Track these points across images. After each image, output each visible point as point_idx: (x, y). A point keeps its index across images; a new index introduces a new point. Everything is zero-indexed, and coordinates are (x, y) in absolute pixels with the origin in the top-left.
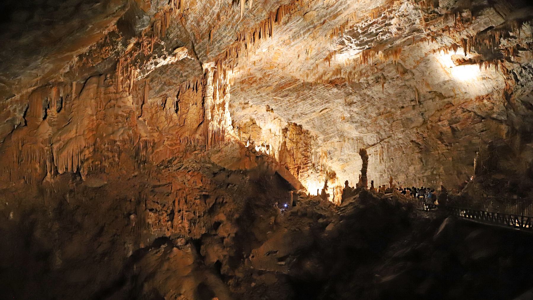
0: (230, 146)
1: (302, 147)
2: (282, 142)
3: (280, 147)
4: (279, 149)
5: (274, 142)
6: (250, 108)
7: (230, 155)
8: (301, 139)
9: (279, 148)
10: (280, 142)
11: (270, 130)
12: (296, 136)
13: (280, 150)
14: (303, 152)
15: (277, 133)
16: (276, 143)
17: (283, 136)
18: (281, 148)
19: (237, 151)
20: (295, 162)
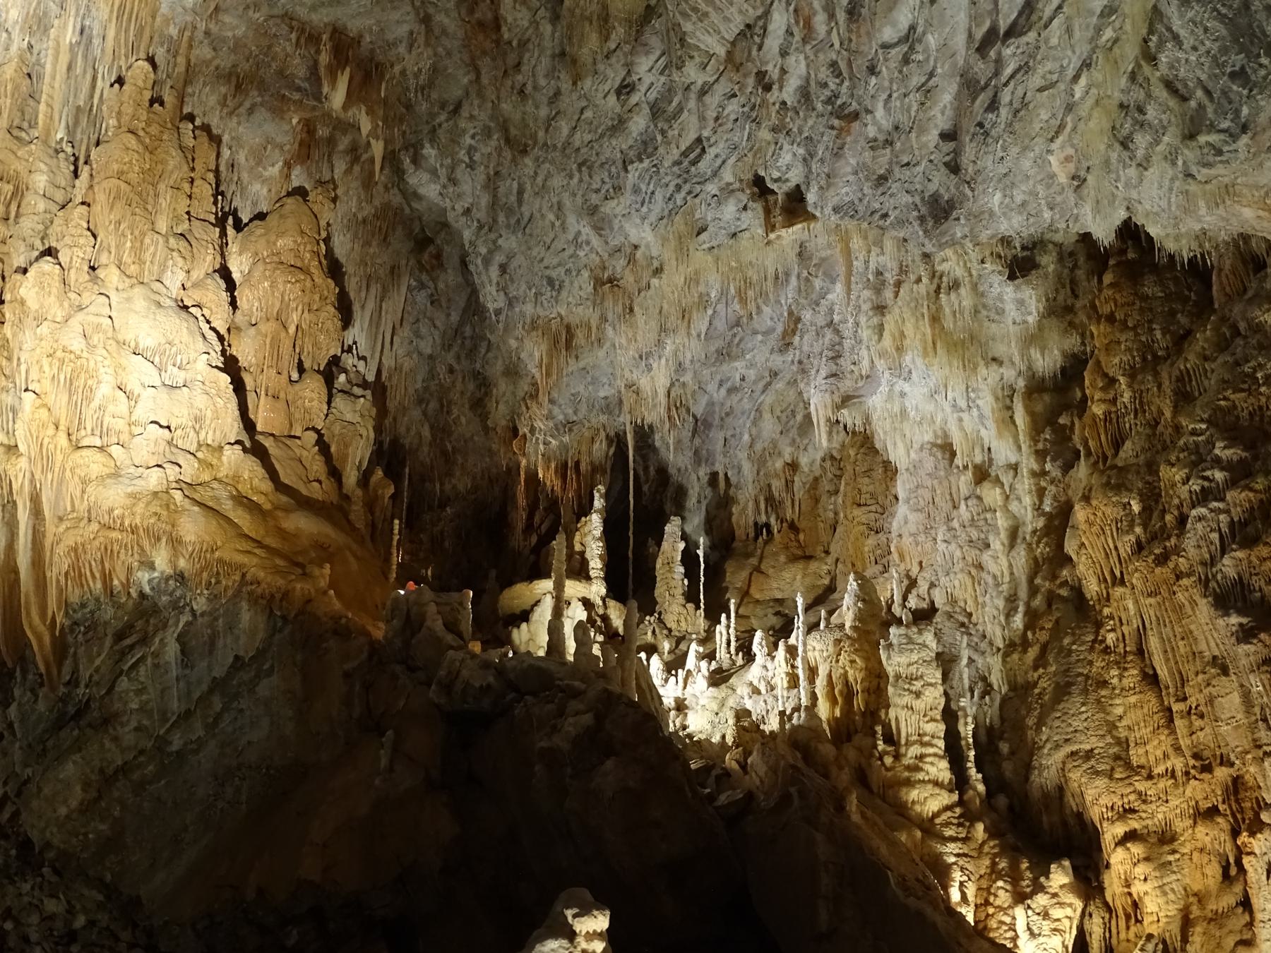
0: (172, 650)
1: (1204, 497)
2: (1032, 522)
3: (1023, 593)
4: (1009, 613)
5: (972, 554)
6: (655, 282)
7: (200, 743)
8: (1183, 398)
9: (1012, 600)
10: (1014, 534)
11: (948, 450)
12: (1139, 396)
13: (1018, 621)
14: (1228, 566)
15: (1004, 452)
16: (986, 558)
17: (1041, 455)
18: (1033, 591)
19: (263, 689)
20: (1179, 723)
